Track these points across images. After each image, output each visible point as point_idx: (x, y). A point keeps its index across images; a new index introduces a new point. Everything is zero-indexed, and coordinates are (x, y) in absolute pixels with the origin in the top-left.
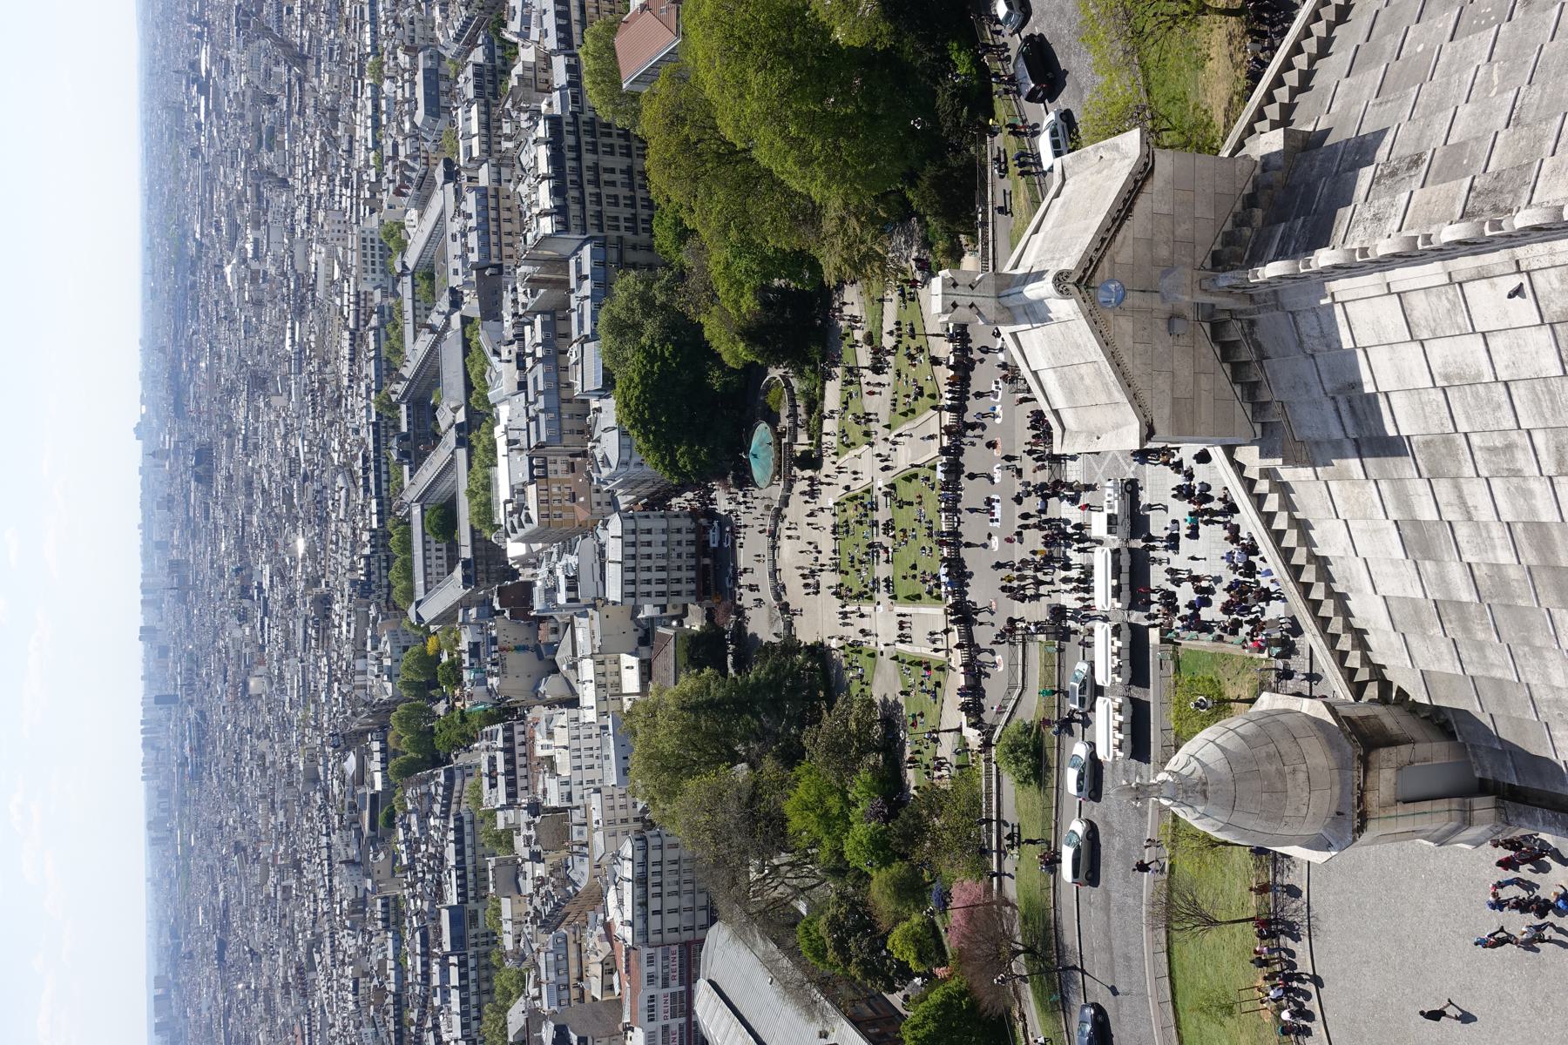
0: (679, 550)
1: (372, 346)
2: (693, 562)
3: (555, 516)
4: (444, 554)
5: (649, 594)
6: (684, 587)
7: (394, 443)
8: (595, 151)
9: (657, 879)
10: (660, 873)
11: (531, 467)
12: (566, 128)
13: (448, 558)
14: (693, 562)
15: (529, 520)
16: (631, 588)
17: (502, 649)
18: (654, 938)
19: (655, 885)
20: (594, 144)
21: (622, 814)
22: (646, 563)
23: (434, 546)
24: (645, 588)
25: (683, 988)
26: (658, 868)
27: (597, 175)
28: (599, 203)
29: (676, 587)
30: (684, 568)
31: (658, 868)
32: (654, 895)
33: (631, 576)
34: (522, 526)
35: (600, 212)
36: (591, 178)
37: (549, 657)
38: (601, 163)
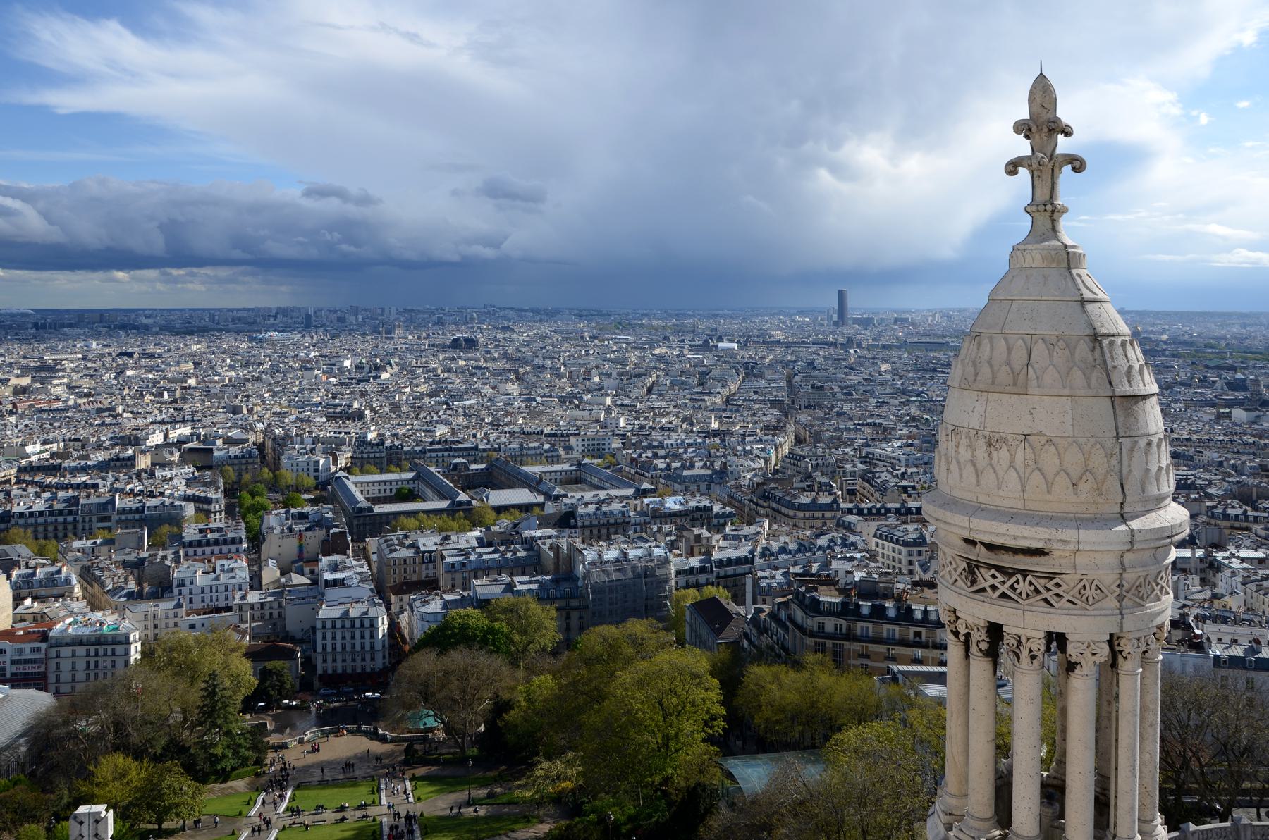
1: (531, 445)
3: (395, 570)
4: (382, 494)
6: (330, 664)
7: (463, 460)
9: (101, 652)
10: (105, 655)
11: (430, 552)
13: (379, 498)
15: (392, 551)
17: (301, 535)
18: (53, 652)
19: (97, 651)
21: (162, 625)
22: (348, 636)
23: (388, 487)
25: (8, 676)
26: (109, 653)
29: (330, 658)
31: (109, 653)
32: (88, 651)
34: (388, 546)
37: (293, 569)
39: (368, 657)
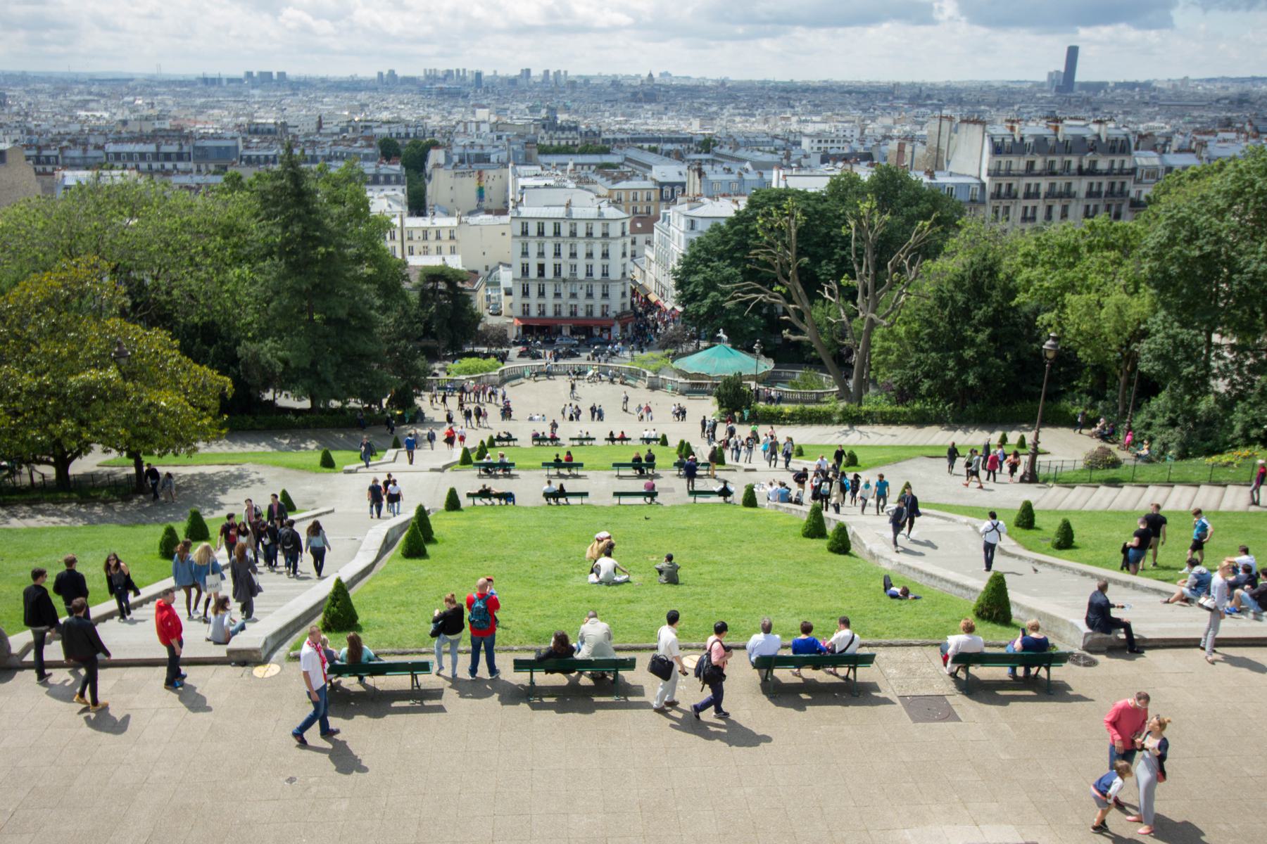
0: (582, 294)
2: (565, 313)
5: (525, 254)
6: (533, 300)
8: (1090, 194)
12: (1117, 160)
14: (565, 313)
16: (533, 230)
20: (1098, 194)
24: (533, 249)
27: (1060, 196)
28: (1028, 196)
29: (534, 291)
30: (558, 301)
33: (549, 230)
35: (1015, 197)
36: (1057, 189)
38: (1074, 202)
39: (597, 291)
